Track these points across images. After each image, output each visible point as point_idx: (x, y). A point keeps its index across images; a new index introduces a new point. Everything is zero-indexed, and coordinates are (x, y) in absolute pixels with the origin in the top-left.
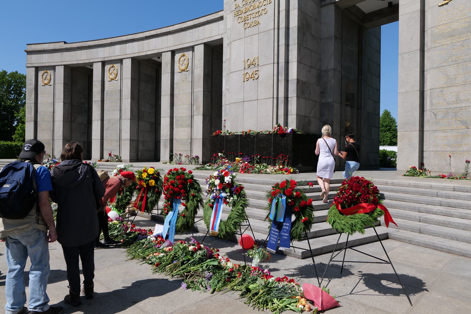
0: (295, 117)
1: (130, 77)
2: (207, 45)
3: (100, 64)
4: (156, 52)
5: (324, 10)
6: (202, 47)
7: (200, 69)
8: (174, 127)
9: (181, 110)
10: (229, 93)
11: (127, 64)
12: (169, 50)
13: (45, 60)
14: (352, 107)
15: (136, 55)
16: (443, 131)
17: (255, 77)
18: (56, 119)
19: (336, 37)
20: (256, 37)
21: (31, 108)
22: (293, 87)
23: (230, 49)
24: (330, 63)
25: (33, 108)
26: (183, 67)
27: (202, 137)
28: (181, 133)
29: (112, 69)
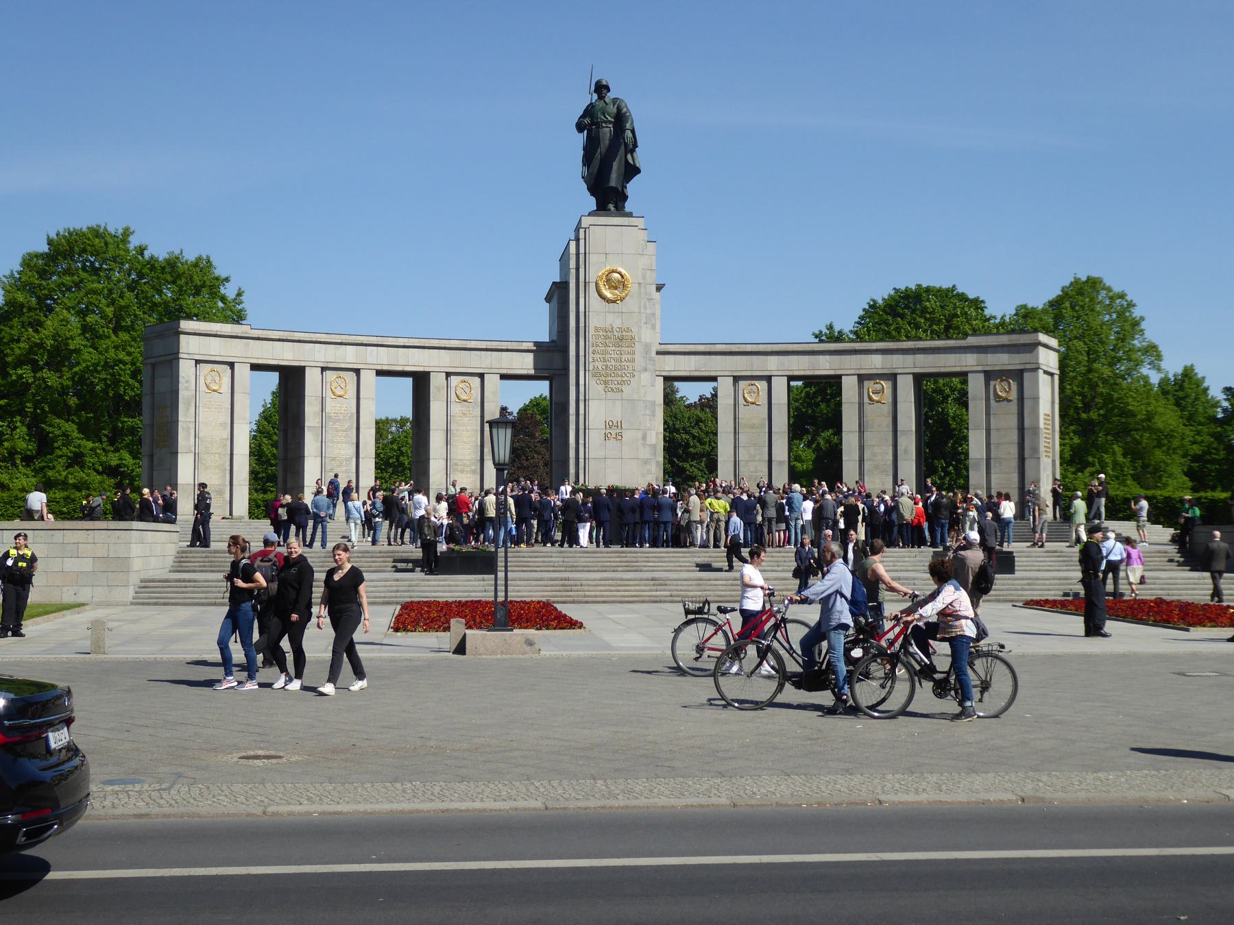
4: (421, 369)
15: (385, 368)
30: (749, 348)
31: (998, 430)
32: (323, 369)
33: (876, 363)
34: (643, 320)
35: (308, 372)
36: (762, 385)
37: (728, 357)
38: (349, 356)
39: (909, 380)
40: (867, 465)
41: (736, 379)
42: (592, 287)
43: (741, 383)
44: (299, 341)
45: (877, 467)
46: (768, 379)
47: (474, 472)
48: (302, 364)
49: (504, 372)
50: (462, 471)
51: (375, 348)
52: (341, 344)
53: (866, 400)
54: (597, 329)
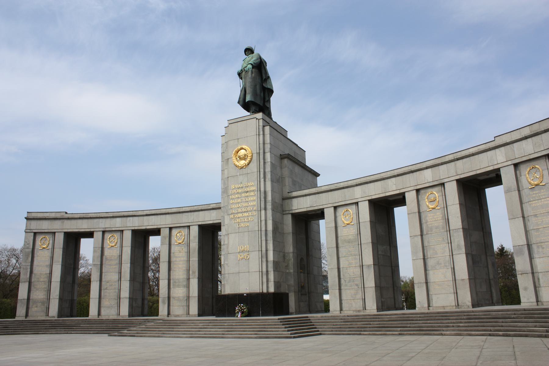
0: (273, 283)
1: (130, 245)
2: (200, 226)
3: (101, 233)
4: (155, 227)
5: (285, 216)
6: (196, 228)
7: (195, 244)
8: (172, 286)
12: (168, 226)
13: (45, 226)
14: (304, 273)
16: (349, 289)
18: (53, 279)
19: (293, 233)
20: (246, 234)
21: (27, 269)
22: (271, 265)
23: (228, 238)
24: (290, 248)
25: (29, 270)
26: (180, 241)
28: (178, 292)
29: (112, 239)
30: (342, 185)
31: (535, 216)
32: (104, 232)
33: (428, 177)
34: (262, 176)
35: (95, 234)
37: (330, 193)
38: (118, 223)
39: (455, 183)
40: (430, 263)
44: (91, 218)
45: (438, 263)
46: (357, 203)
47: (184, 286)
48: (92, 230)
49: (200, 223)
51: (131, 218)
52: (113, 217)
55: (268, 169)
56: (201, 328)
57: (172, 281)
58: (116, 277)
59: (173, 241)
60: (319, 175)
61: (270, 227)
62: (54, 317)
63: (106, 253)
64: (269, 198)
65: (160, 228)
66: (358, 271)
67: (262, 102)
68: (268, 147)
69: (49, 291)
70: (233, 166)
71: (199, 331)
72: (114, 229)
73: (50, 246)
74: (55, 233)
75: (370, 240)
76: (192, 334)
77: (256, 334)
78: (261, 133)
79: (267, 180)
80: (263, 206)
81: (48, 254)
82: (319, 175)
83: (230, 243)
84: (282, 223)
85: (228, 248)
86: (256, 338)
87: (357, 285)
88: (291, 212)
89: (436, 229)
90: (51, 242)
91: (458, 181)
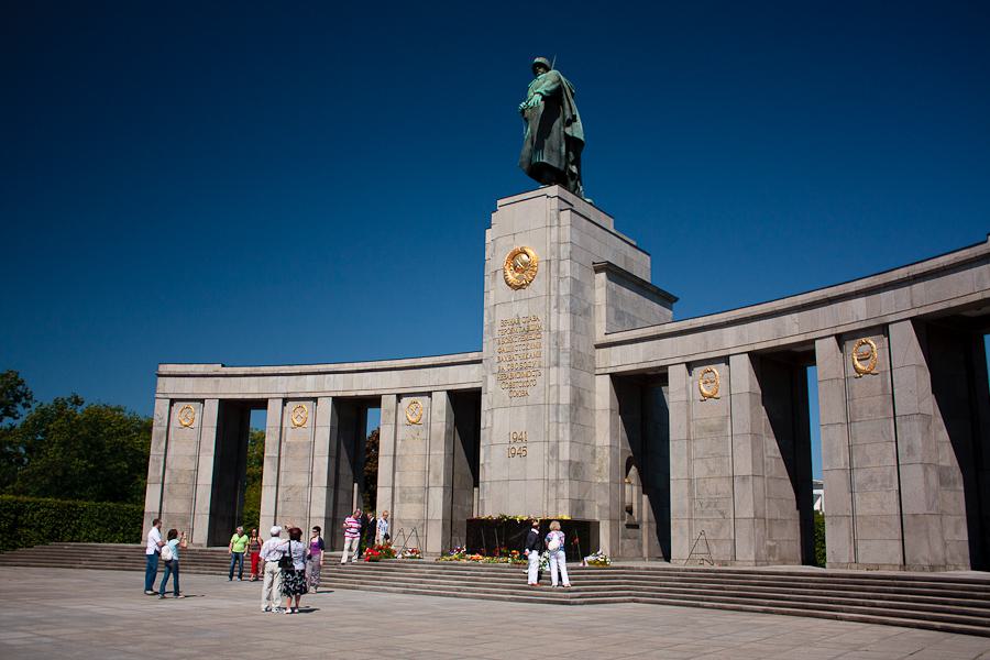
4: (372, 393)
6: (444, 396)
9: (411, 478)
10: (491, 468)
11: (326, 406)
15: (339, 394)
16: (708, 520)
17: (522, 454)
20: (523, 409)
21: (158, 461)
22: (563, 469)
25: (162, 463)
26: (413, 420)
27: (441, 518)
34: (553, 304)
36: (718, 370)
40: (859, 477)
41: (690, 366)
42: (500, 275)
43: (697, 371)
45: (871, 480)
46: (726, 360)
48: (265, 396)
50: (410, 500)
51: (332, 376)
52: (301, 374)
53: (852, 372)
54: (504, 323)
55: (565, 289)
56: (427, 578)
57: (397, 491)
58: (303, 480)
59: (399, 422)
60: (676, 299)
61: (565, 398)
62: (201, 545)
63: (289, 435)
64: (567, 345)
65: (381, 395)
66: (725, 486)
67: (563, 164)
68: (565, 250)
69: (193, 500)
70: (504, 283)
71: (421, 582)
72: (302, 395)
73: (196, 424)
74: (202, 401)
75: (748, 428)
76: (408, 587)
77: (512, 594)
78: (556, 222)
79: (563, 311)
80: (553, 359)
81: (191, 434)
82: (676, 299)
83: (495, 423)
84: (591, 391)
85: (491, 434)
86: (510, 600)
87: (722, 513)
88: (609, 371)
89: (870, 411)
90: (197, 416)
91: (917, 322)
